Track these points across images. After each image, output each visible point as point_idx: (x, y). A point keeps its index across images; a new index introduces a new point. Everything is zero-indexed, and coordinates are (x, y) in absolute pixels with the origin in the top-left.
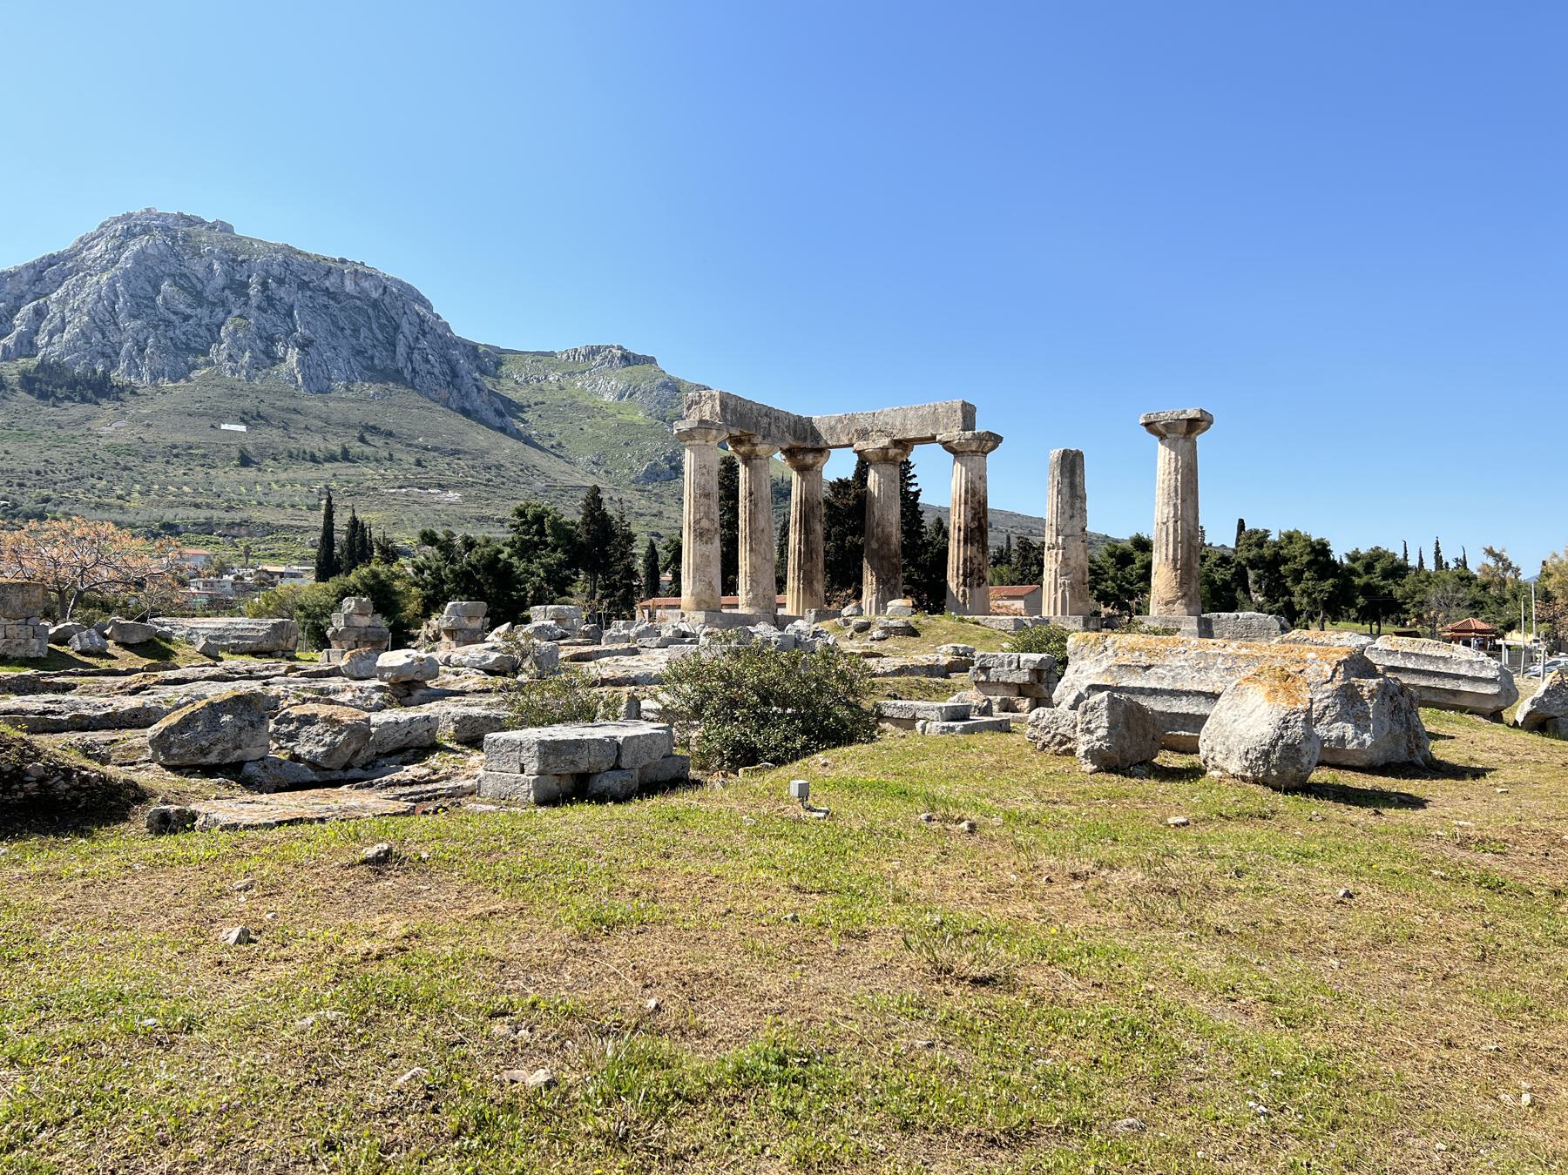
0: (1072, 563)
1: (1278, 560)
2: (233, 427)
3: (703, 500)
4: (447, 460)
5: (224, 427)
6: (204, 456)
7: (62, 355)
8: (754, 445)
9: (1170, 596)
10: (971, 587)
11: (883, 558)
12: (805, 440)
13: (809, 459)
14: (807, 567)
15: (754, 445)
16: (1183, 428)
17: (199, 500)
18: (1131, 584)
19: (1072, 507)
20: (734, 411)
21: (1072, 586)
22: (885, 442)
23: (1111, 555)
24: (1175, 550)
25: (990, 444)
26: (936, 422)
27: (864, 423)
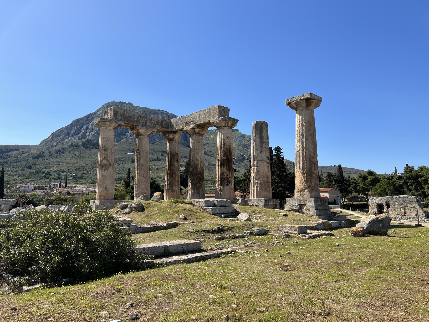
0: (261, 173)
1: (418, 177)
2: (130, 153)
3: (104, 152)
4: (183, 159)
5: (128, 153)
6: (123, 161)
7: (92, 138)
8: (138, 130)
9: (301, 187)
10: (223, 186)
11: (194, 175)
12: (168, 128)
13: (171, 136)
14: (170, 180)
15: (138, 130)
16: (304, 104)
17: (120, 172)
18: (367, 186)
19: (261, 147)
20: (123, 115)
21: (261, 184)
22: (192, 126)
23: (360, 177)
24: (303, 164)
25: (230, 123)
26: (210, 115)
27: (187, 119)
